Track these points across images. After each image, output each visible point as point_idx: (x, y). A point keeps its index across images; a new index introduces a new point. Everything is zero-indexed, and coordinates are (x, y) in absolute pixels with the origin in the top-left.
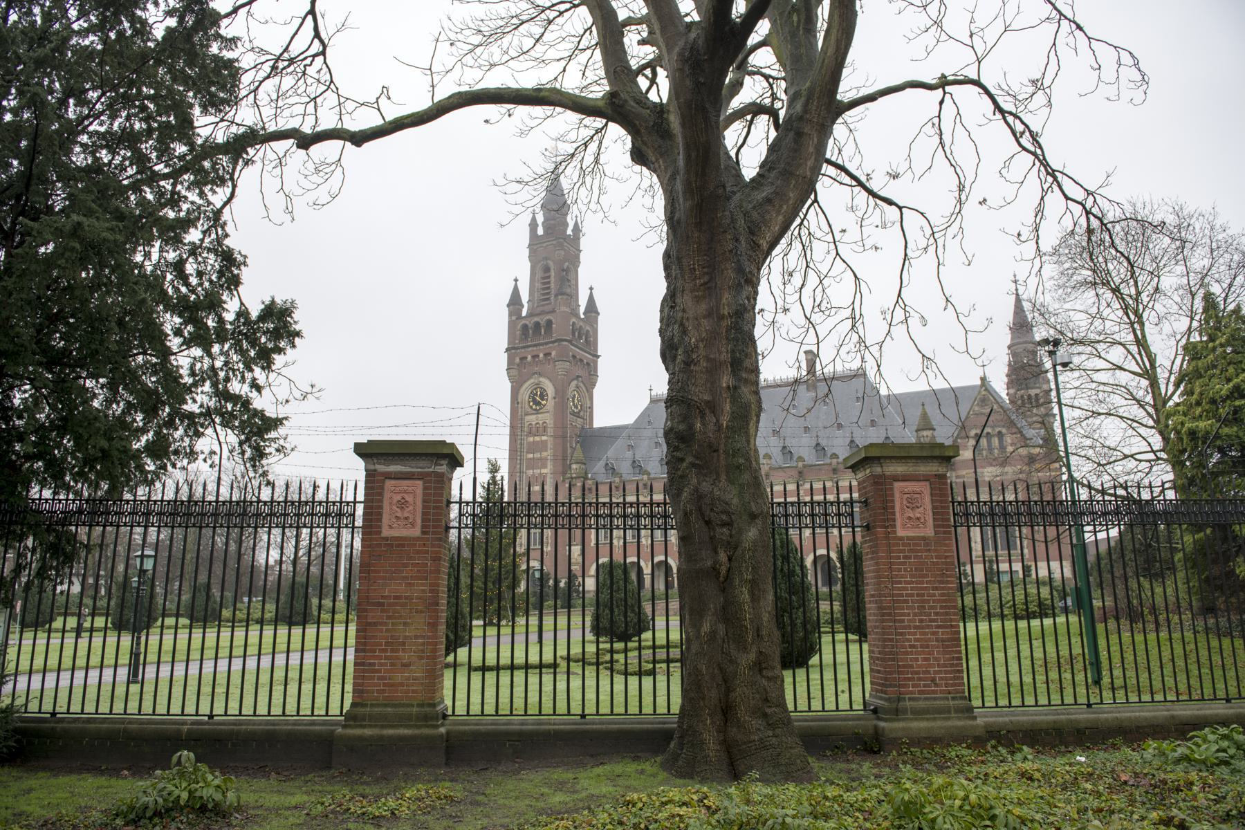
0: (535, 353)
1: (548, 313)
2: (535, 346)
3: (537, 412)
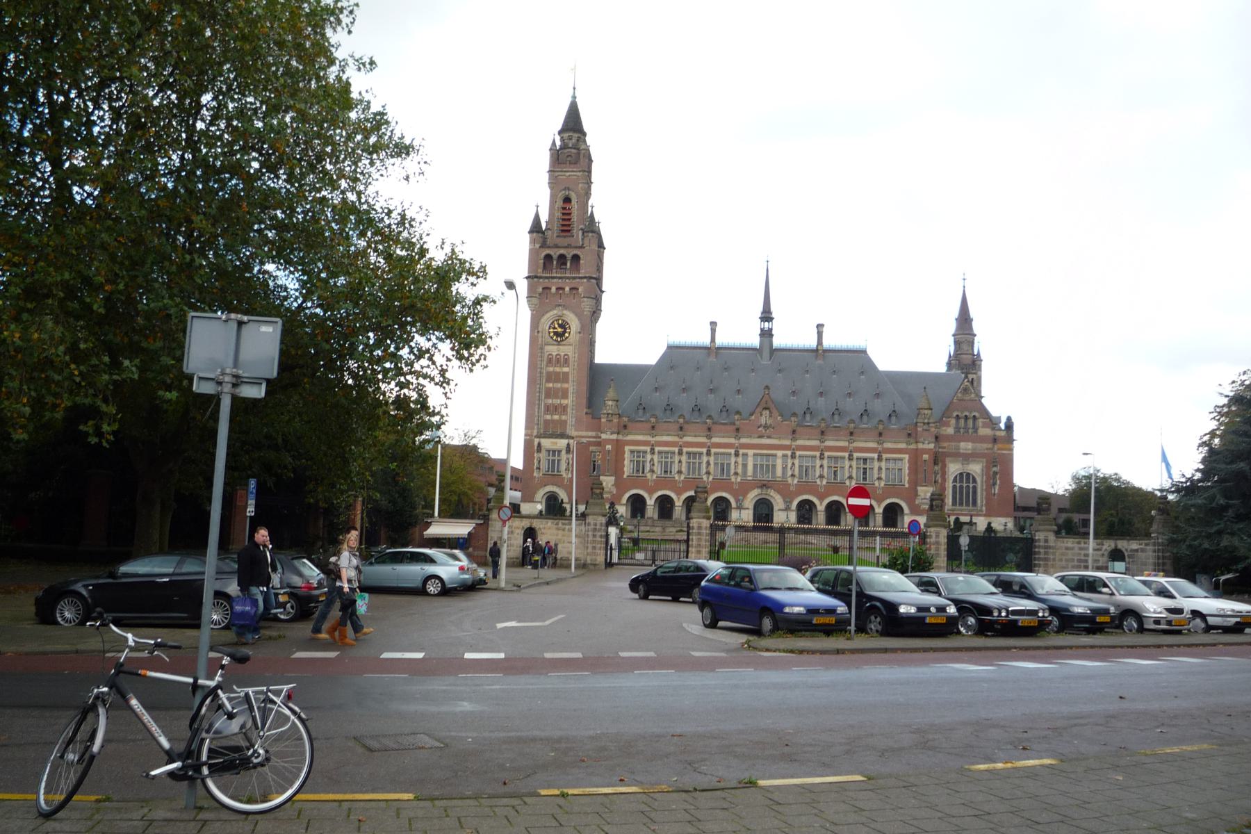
0: (560, 286)
1: (576, 247)
2: (560, 278)
3: (559, 343)
